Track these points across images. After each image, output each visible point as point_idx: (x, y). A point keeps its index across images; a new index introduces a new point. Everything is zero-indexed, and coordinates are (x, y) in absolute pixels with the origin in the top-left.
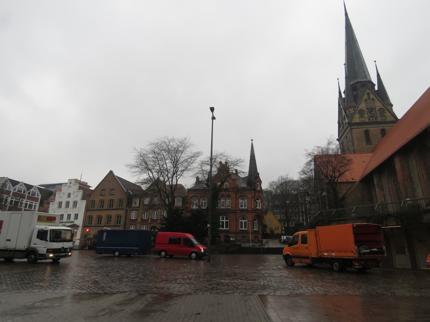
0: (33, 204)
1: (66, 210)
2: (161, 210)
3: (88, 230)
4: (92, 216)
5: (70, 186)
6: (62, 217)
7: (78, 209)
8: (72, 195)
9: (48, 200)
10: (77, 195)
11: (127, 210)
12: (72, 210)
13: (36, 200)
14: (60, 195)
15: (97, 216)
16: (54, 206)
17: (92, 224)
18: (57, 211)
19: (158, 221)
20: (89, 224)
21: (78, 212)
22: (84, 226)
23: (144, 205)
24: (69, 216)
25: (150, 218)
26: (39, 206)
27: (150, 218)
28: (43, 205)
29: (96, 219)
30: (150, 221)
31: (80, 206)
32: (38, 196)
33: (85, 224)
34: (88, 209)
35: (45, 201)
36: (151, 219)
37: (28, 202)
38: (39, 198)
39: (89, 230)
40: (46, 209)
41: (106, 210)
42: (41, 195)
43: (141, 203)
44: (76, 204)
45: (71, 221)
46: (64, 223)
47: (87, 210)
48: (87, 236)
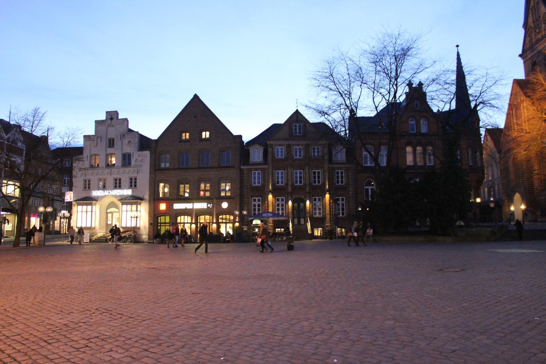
1: (109, 170)
2: (309, 169)
6: (257, 178)
7: (136, 169)
8: (117, 143)
11: (241, 171)
19: (307, 189)
23: (274, 160)
25: (290, 183)
27: (290, 183)
30: (290, 189)
34: (157, 168)
36: (291, 185)
43: (270, 157)
44: (130, 159)
47: (155, 170)
48: (199, 217)
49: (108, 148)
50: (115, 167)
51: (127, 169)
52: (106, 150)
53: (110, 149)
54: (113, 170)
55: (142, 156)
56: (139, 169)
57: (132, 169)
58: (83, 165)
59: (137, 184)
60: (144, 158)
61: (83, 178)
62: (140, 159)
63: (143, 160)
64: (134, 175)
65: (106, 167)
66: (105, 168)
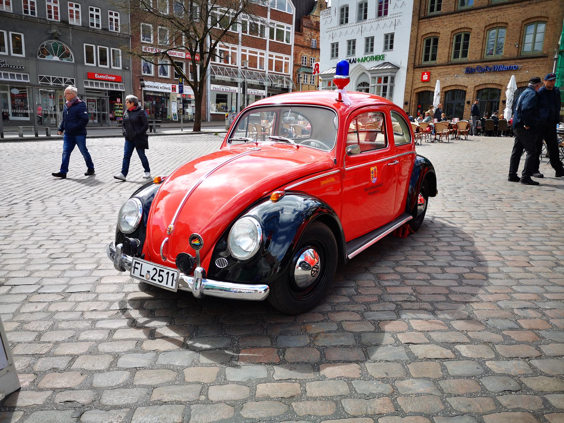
0: (282, 29)
3: (425, 77)
4: (438, 35)
9: (309, 18)
12: (375, 24)
13: (286, 18)
15: (452, 32)
17: (437, 57)
18: (338, 32)
20: (426, 59)
21: (393, 27)
22: (414, 66)
24: (370, 42)
26: (295, 34)
28: (302, 31)
29: (451, 43)
31: (398, 10)
32: (289, 9)
33: (417, 61)
34: (422, 15)
35: (305, 22)
38: (292, 15)
39: (429, 77)
40: (309, 39)
41: (486, 10)
42: (295, 8)
45: (376, 56)
46: (360, 63)
47: (420, 19)
50: (367, 21)
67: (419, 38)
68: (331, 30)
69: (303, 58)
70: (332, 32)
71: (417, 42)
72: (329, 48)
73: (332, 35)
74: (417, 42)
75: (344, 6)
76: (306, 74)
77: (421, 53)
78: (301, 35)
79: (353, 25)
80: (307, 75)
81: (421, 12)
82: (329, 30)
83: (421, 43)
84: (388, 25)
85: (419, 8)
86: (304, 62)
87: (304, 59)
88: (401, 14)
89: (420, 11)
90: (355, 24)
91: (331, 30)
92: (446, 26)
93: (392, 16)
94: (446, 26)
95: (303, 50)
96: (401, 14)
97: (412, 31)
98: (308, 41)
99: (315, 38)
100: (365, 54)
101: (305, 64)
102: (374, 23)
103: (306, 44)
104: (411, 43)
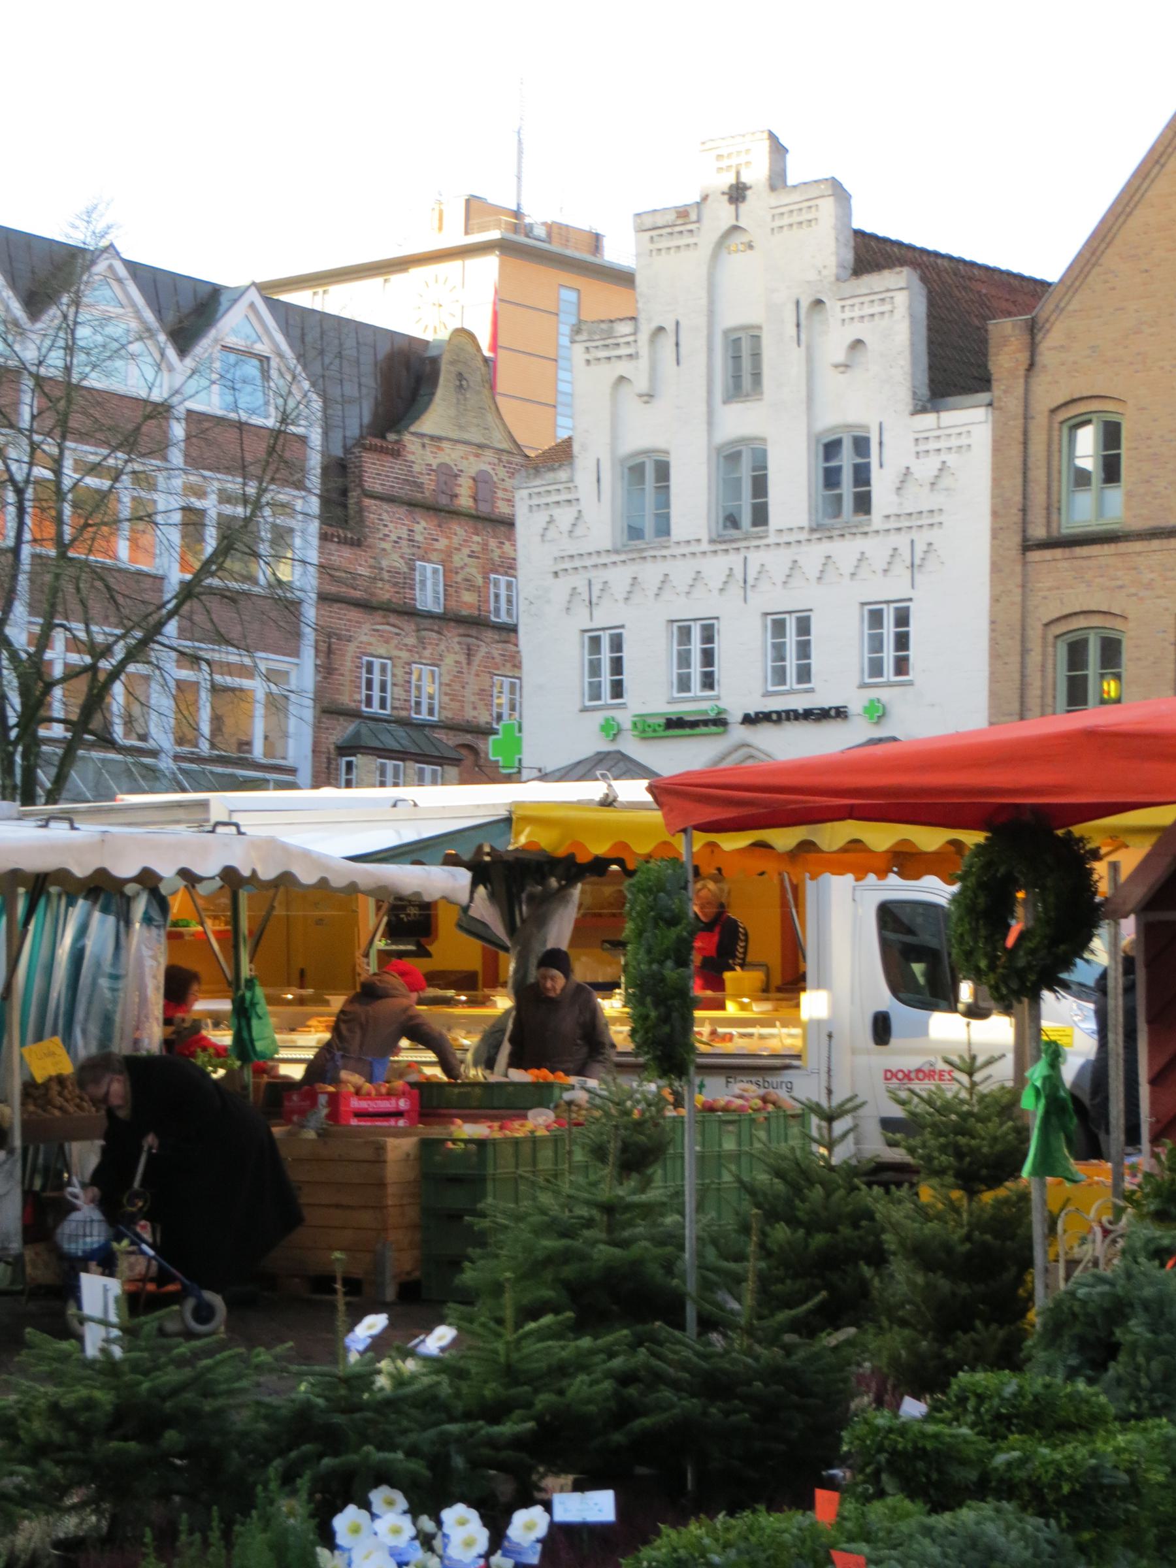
4: (1118, 624)
5: (736, 228)
7: (901, 541)
9: (396, 452)
10: (858, 344)
14: (622, 368)
16: (565, 516)
18: (619, 577)
21: (900, 569)
28: (361, 521)
31: (919, 499)
34: (1039, 532)
37: (201, 494)
40: (401, 565)
44: (862, 475)
47: (1028, 546)
49: (727, 400)
50: (771, 540)
51: (845, 550)
52: (710, 423)
53: (736, 408)
54: (756, 558)
55: (942, 444)
56: (920, 548)
57: (876, 548)
58: (578, 532)
59: (914, 653)
60: (951, 459)
61: (582, 619)
62: (925, 469)
63: (945, 481)
64: (893, 588)
65: (712, 541)
66: (705, 546)
67: (1035, 633)
68: (577, 563)
69: (370, 667)
70: (588, 575)
71: (1024, 652)
72: (574, 654)
73: (583, 589)
74: (1024, 652)
75: (646, 452)
76: (390, 764)
77: (1049, 700)
78: (357, 543)
79: (694, 548)
80: (396, 768)
81: (1030, 518)
82: (568, 565)
83: (1044, 654)
84: (880, 563)
85: (1018, 498)
86: (376, 694)
87: (376, 677)
88: (936, 519)
89: (1024, 510)
90: (705, 546)
91: (577, 563)
92: (1149, 586)
93: (892, 524)
94: (1149, 586)
95: (366, 628)
96: (936, 519)
97: (995, 600)
98: (394, 572)
99: (434, 556)
100: (767, 694)
101: (383, 705)
102: (805, 548)
103: (385, 593)
104: (995, 655)
